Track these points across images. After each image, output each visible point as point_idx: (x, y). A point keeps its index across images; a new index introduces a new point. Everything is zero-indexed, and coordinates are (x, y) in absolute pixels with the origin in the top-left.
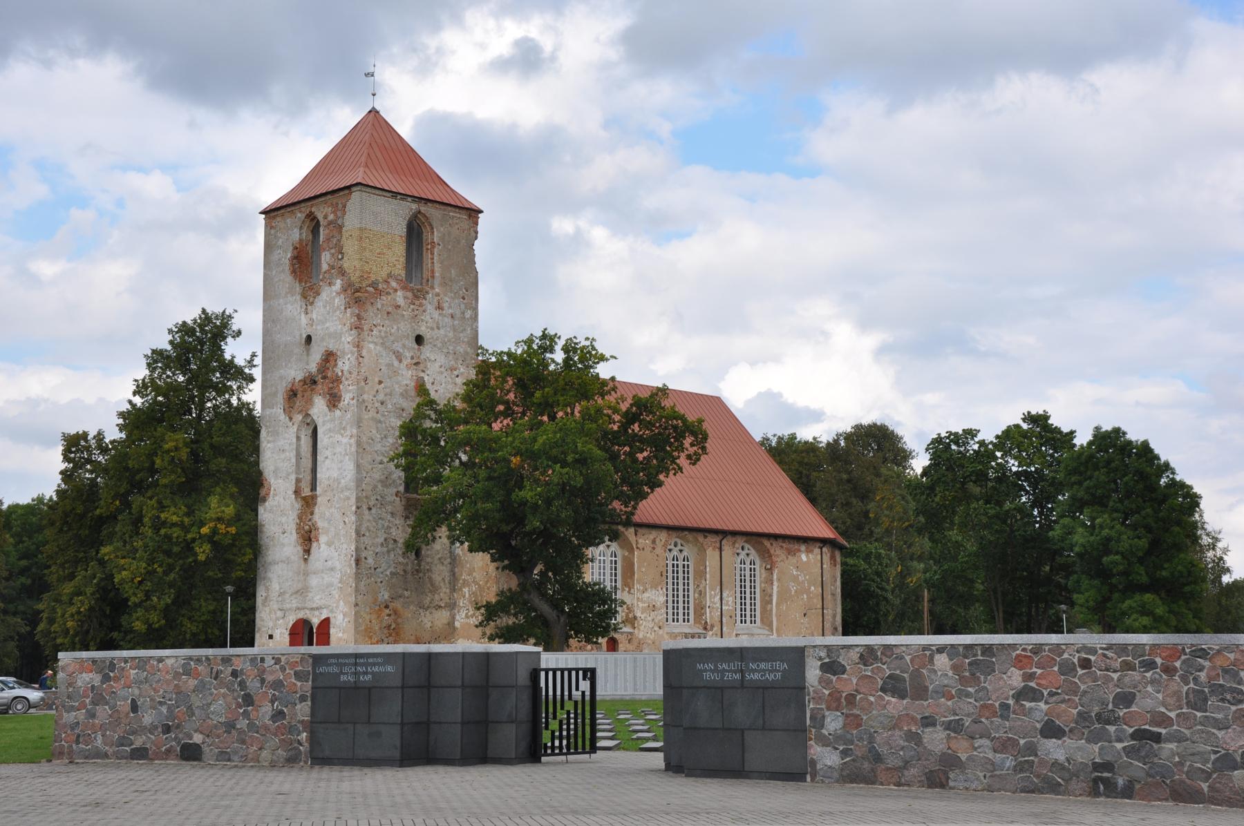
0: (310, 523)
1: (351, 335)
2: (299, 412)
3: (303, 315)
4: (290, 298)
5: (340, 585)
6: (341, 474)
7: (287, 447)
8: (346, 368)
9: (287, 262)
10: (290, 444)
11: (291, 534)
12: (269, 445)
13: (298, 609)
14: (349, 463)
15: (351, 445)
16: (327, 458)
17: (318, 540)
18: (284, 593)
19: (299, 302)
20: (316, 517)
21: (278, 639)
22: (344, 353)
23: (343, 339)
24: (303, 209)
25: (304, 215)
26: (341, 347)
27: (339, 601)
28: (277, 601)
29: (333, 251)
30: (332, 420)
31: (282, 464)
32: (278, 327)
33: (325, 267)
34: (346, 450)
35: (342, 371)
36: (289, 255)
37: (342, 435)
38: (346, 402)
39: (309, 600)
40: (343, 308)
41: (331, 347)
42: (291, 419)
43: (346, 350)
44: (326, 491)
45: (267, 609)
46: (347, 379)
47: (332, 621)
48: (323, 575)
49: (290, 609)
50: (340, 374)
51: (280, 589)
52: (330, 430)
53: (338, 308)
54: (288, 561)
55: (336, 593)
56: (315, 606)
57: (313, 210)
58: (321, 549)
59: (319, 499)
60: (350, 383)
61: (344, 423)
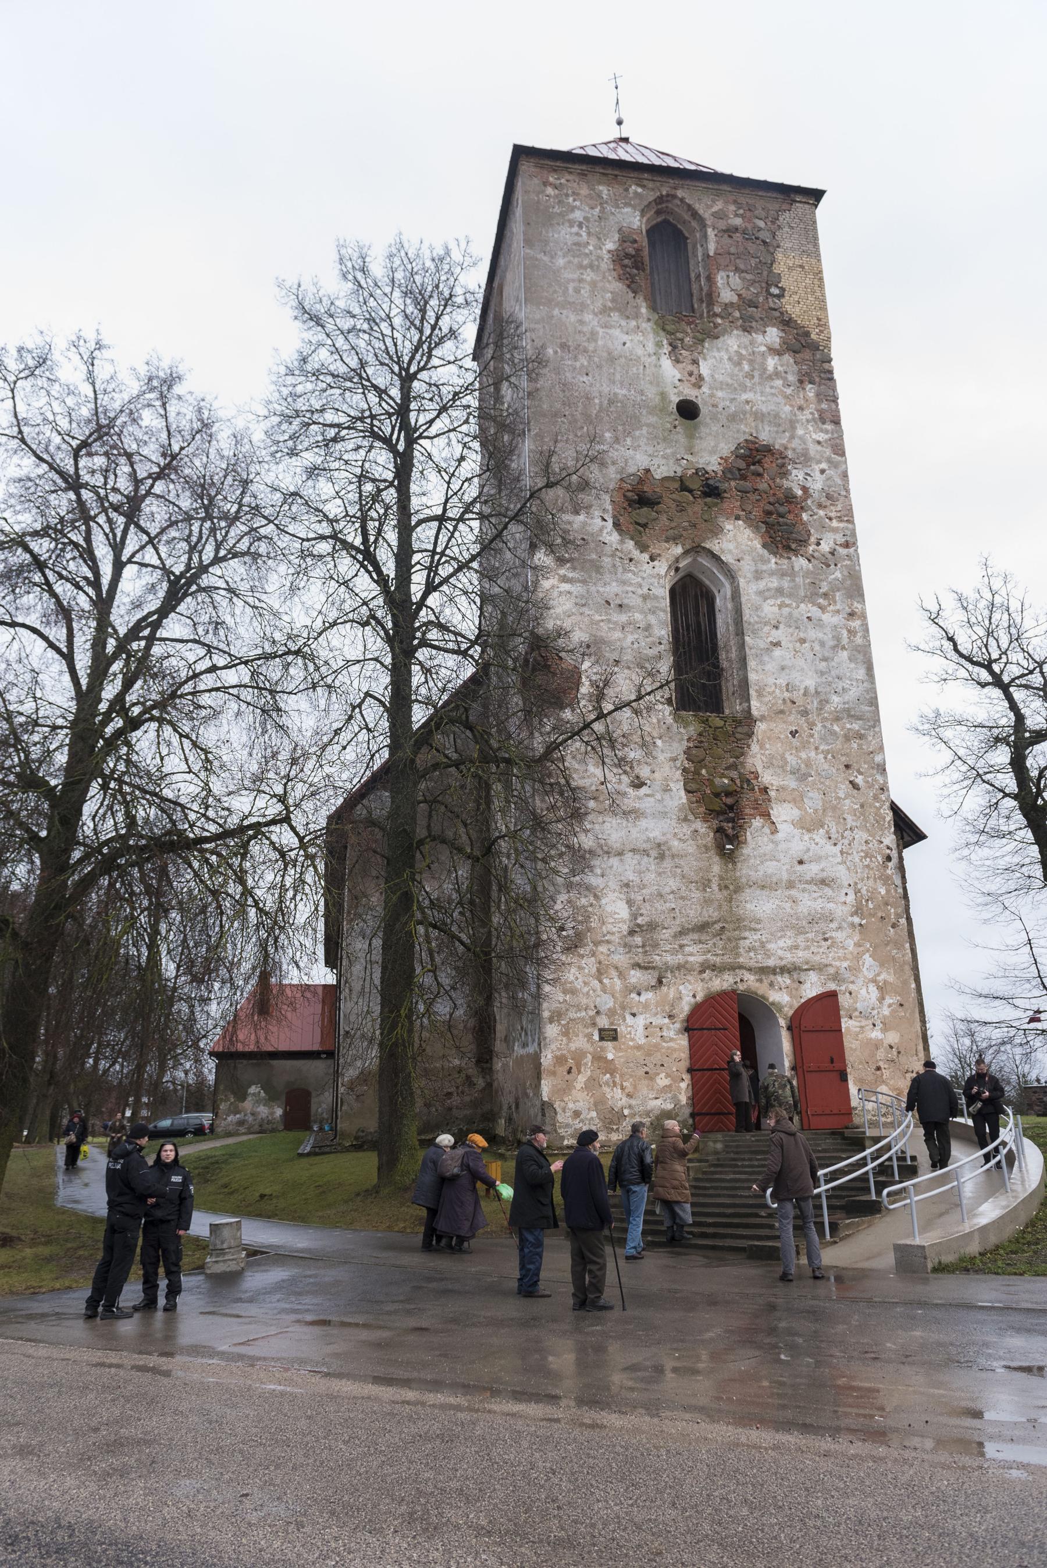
0: (734, 774)
1: (826, 432)
2: (675, 539)
3: (666, 363)
4: (615, 316)
5: (856, 920)
6: (830, 684)
7: (635, 601)
8: (817, 484)
9: (606, 256)
10: (645, 598)
11: (667, 790)
12: (565, 587)
13: (713, 968)
14: (853, 665)
15: (851, 632)
16: (777, 644)
17: (766, 815)
18: (652, 926)
19: (651, 335)
20: (756, 758)
21: (642, 1041)
22: (805, 459)
23: (800, 432)
24: (650, 185)
25: (651, 196)
26: (795, 444)
27: (858, 957)
28: (625, 945)
29: (749, 277)
30: (791, 573)
31: (617, 634)
32: (583, 361)
33: (727, 296)
34: (838, 638)
35: (805, 489)
36: (610, 245)
37: (822, 608)
38: (825, 547)
39: (750, 949)
40: (792, 378)
41: (765, 435)
42: (643, 548)
43: (812, 453)
44: (782, 712)
45: (590, 964)
46: (820, 506)
47: (844, 1001)
48: (793, 892)
49: (679, 967)
50: (800, 493)
51: (634, 916)
52: (780, 591)
53: (777, 374)
54: (661, 852)
55: (848, 940)
56: (771, 962)
57: (680, 193)
58: (780, 836)
59: (761, 727)
60: (833, 515)
61: (825, 588)
